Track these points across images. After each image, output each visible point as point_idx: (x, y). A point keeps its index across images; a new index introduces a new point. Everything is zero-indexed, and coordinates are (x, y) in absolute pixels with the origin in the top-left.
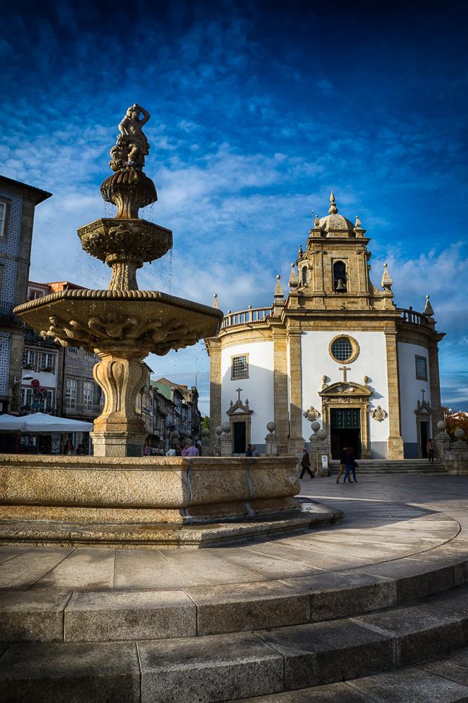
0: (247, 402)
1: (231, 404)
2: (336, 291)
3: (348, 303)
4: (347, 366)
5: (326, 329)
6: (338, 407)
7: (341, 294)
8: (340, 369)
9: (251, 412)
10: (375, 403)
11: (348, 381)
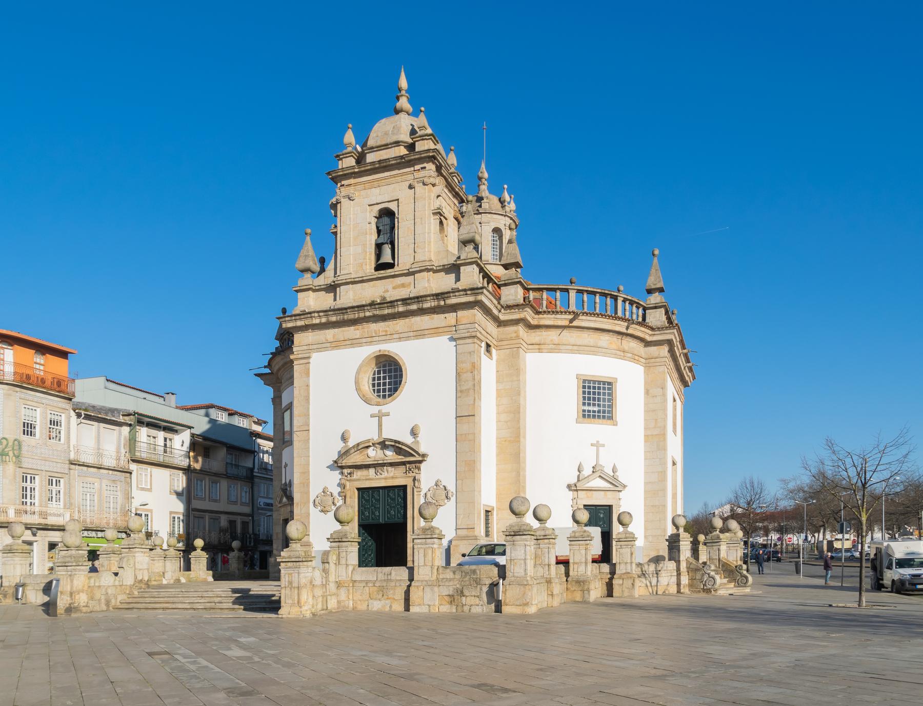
2: (323, 270)
3: (394, 288)
4: (384, 409)
5: (354, 343)
11: (386, 435)
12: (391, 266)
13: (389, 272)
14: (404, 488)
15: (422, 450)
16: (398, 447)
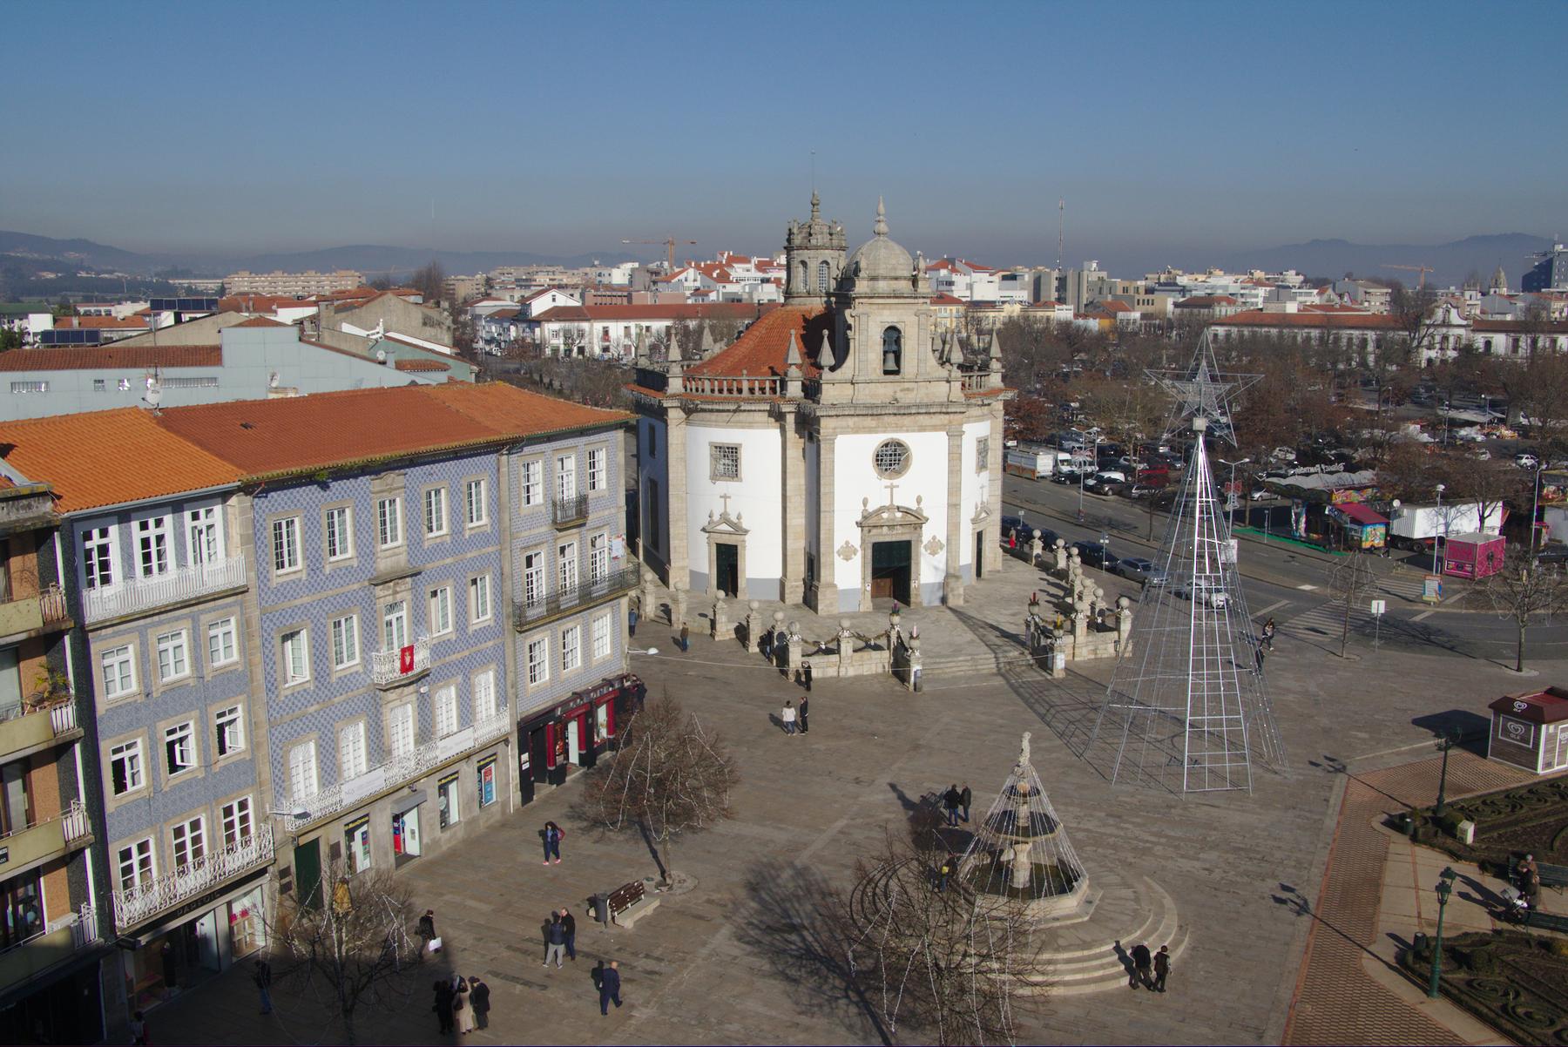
0: (739, 517)
4: (895, 482)
5: (870, 430)
6: (881, 539)
9: (746, 532)
10: (927, 533)
11: (896, 503)
12: (897, 372)
13: (897, 377)
14: (909, 543)
16: (907, 512)
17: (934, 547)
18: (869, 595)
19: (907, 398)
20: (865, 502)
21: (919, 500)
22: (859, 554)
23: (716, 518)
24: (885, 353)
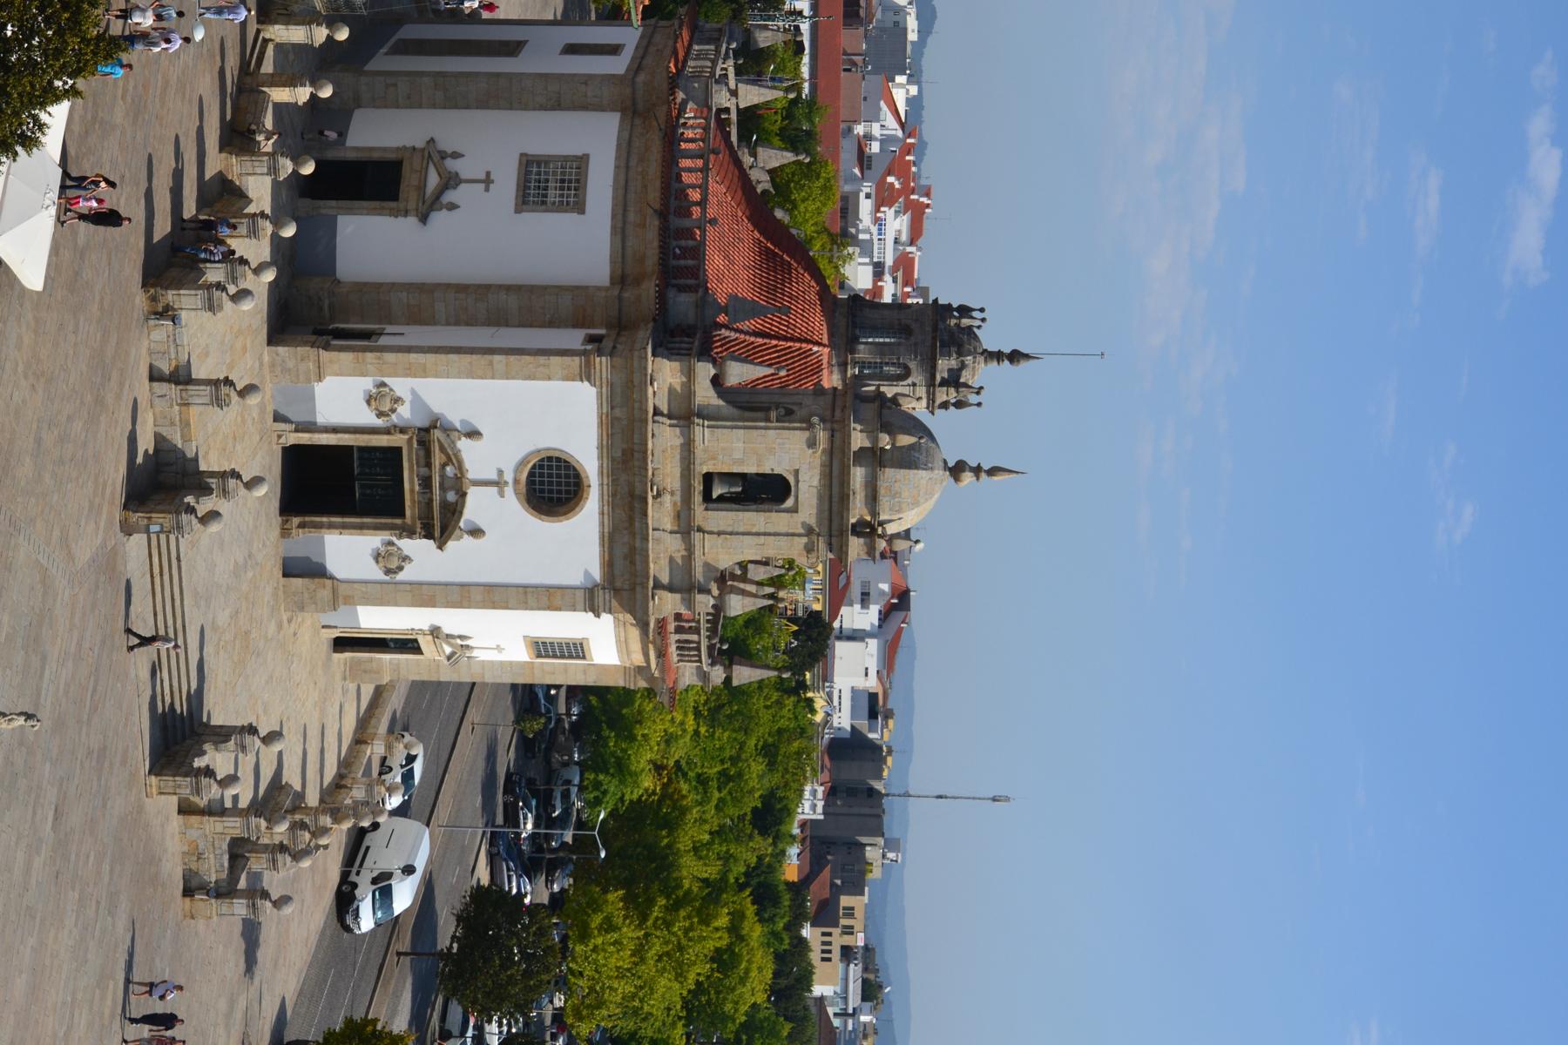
0: (452, 207)
1: (456, 155)
4: (509, 490)
7: (698, 487)
8: (500, 472)
9: (424, 219)
13: (698, 498)
15: (450, 544)
16: (453, 512)
17: (390, 561)
18: (305, 438)
19: (661, 514)
20: (473, 434)
21: (476, 532)
22: (379, 422)
23: (451, 164)
24: (743, 476)
